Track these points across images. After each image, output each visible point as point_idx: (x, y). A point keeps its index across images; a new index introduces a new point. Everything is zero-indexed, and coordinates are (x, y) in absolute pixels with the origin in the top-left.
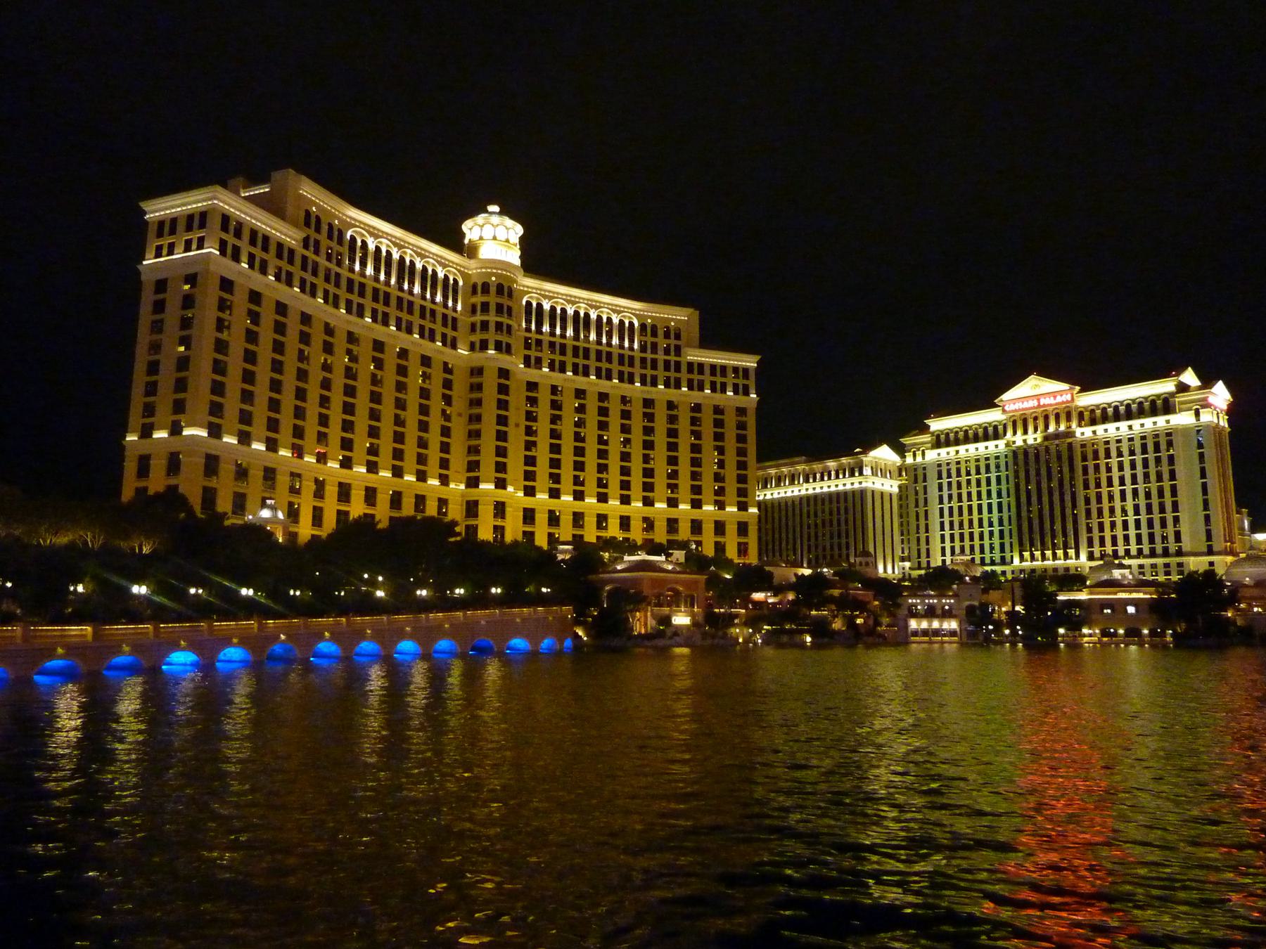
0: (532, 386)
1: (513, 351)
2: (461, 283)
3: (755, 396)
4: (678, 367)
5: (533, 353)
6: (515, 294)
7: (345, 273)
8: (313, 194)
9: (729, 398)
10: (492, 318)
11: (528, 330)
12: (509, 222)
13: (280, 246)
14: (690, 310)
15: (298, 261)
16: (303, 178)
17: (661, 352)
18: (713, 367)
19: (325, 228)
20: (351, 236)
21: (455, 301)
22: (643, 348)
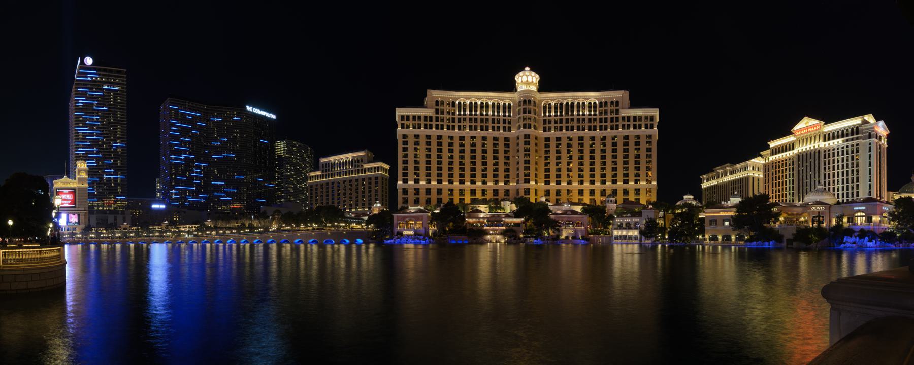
0: (547, 139)
1: (532, 127)
2: (512, 105)
3: (655, 129)
4: (617, 119)
5: (547, 125)
6: (532, 103)
7: (456, 117)
8: (436, 94)
9: (643, 131)
10: (522, 115)
11: (545, 116)
12: (533, 74)
13: (426, 117)
14: (622, 92)
15: (434, 119)
16: (432, 91)
17: (609, 113)
18: (635, 117)
19: (445, 104)
20: (459, 103)
21: (509, 112)
22: (601, 113)
